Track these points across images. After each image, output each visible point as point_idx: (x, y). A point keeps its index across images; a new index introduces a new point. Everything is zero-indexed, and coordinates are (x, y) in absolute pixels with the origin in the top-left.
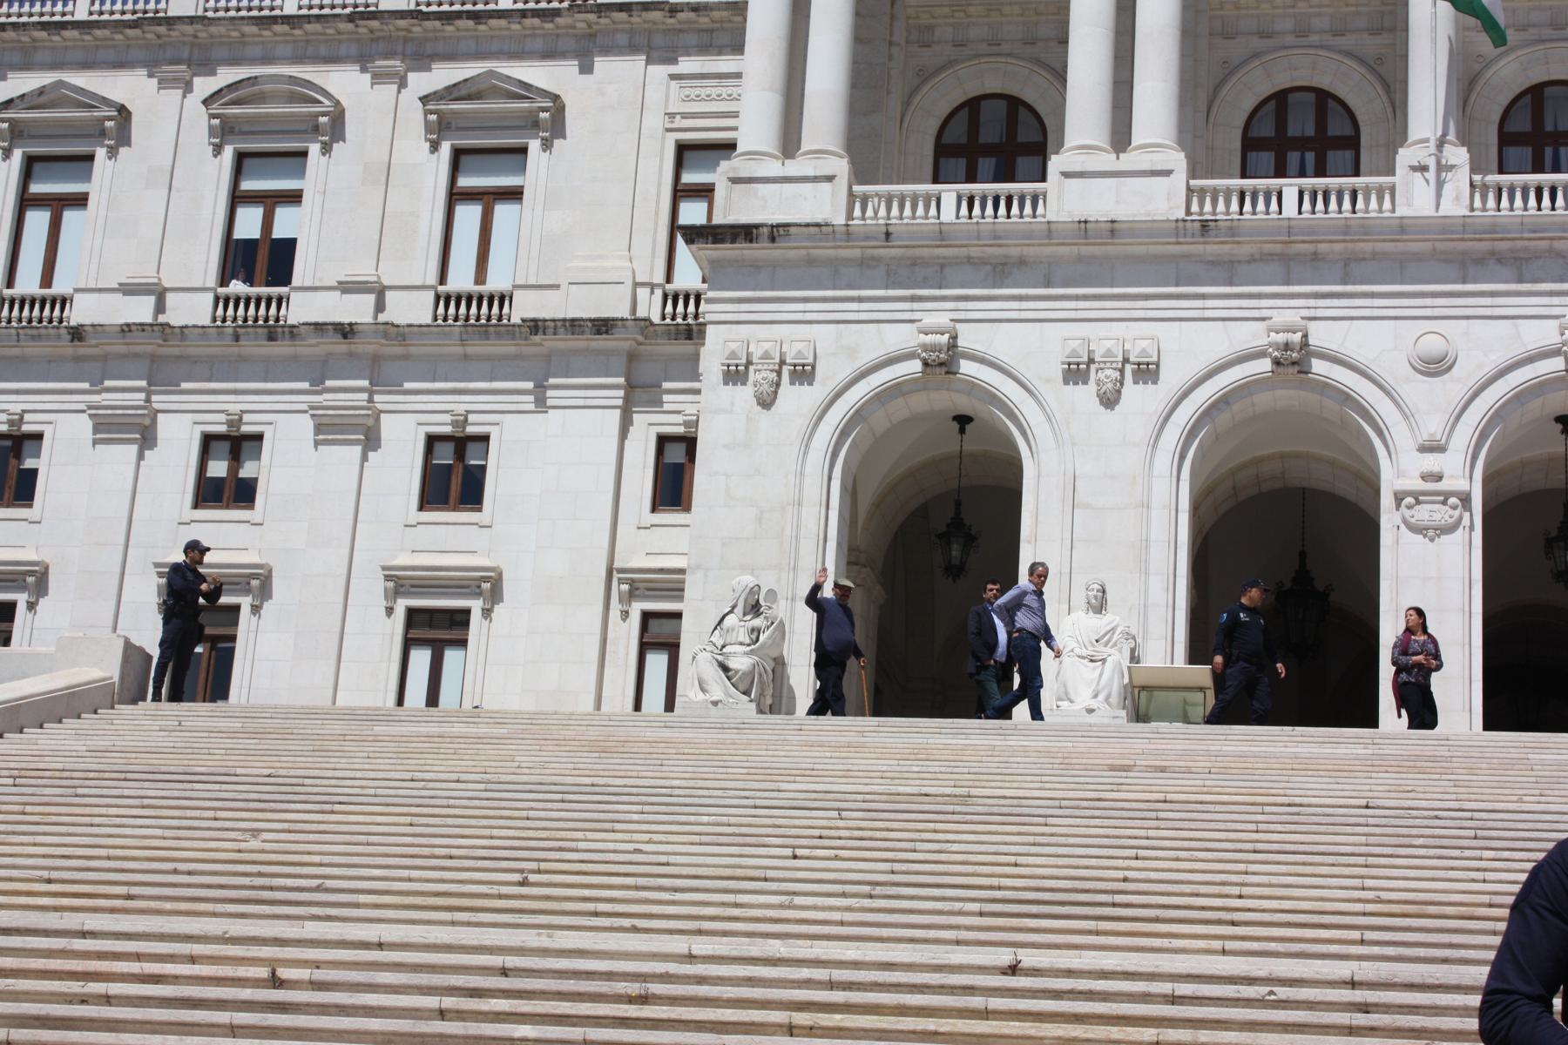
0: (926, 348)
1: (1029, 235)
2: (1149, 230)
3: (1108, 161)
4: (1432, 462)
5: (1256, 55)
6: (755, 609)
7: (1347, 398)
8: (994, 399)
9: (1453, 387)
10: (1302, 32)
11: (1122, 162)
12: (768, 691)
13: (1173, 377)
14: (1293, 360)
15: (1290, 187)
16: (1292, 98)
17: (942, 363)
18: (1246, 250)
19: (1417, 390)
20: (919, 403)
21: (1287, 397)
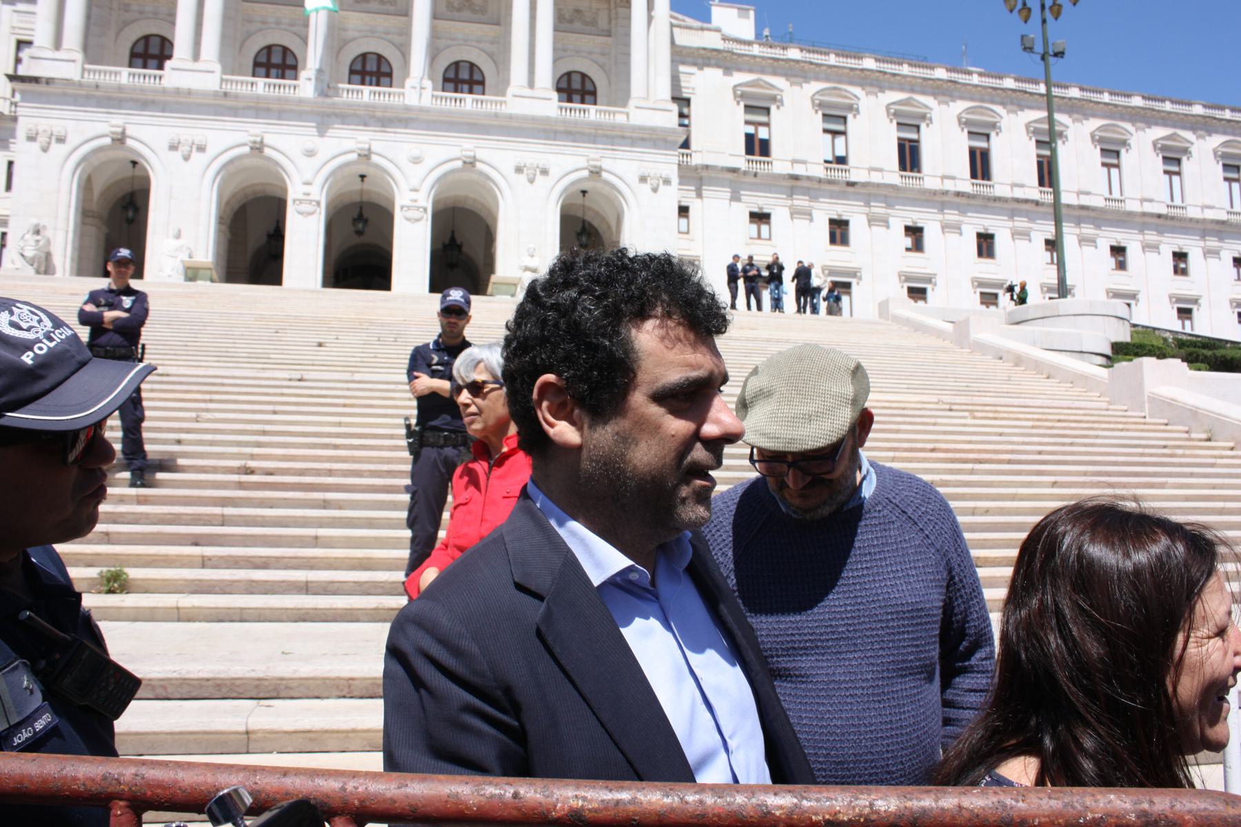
0: (113, 133)
1: (155, 91)
2: (204, 94)
3: (191, 65)
4: (307, 189)
5: (260, 30)
6: (37, 232)
7: (277, 163)
8: (141, 155)
9: (317, 161)
10: (278, 23)
11: (196, 66)
12: (45, 266)
13: (211, 151)
14: (258, 148)
15: (261, 82)
16: (274, 49)
17: (120, 140)
18: (241, 104)
19: (304, 162)
20: (112, 154)
21: (255, 161)
